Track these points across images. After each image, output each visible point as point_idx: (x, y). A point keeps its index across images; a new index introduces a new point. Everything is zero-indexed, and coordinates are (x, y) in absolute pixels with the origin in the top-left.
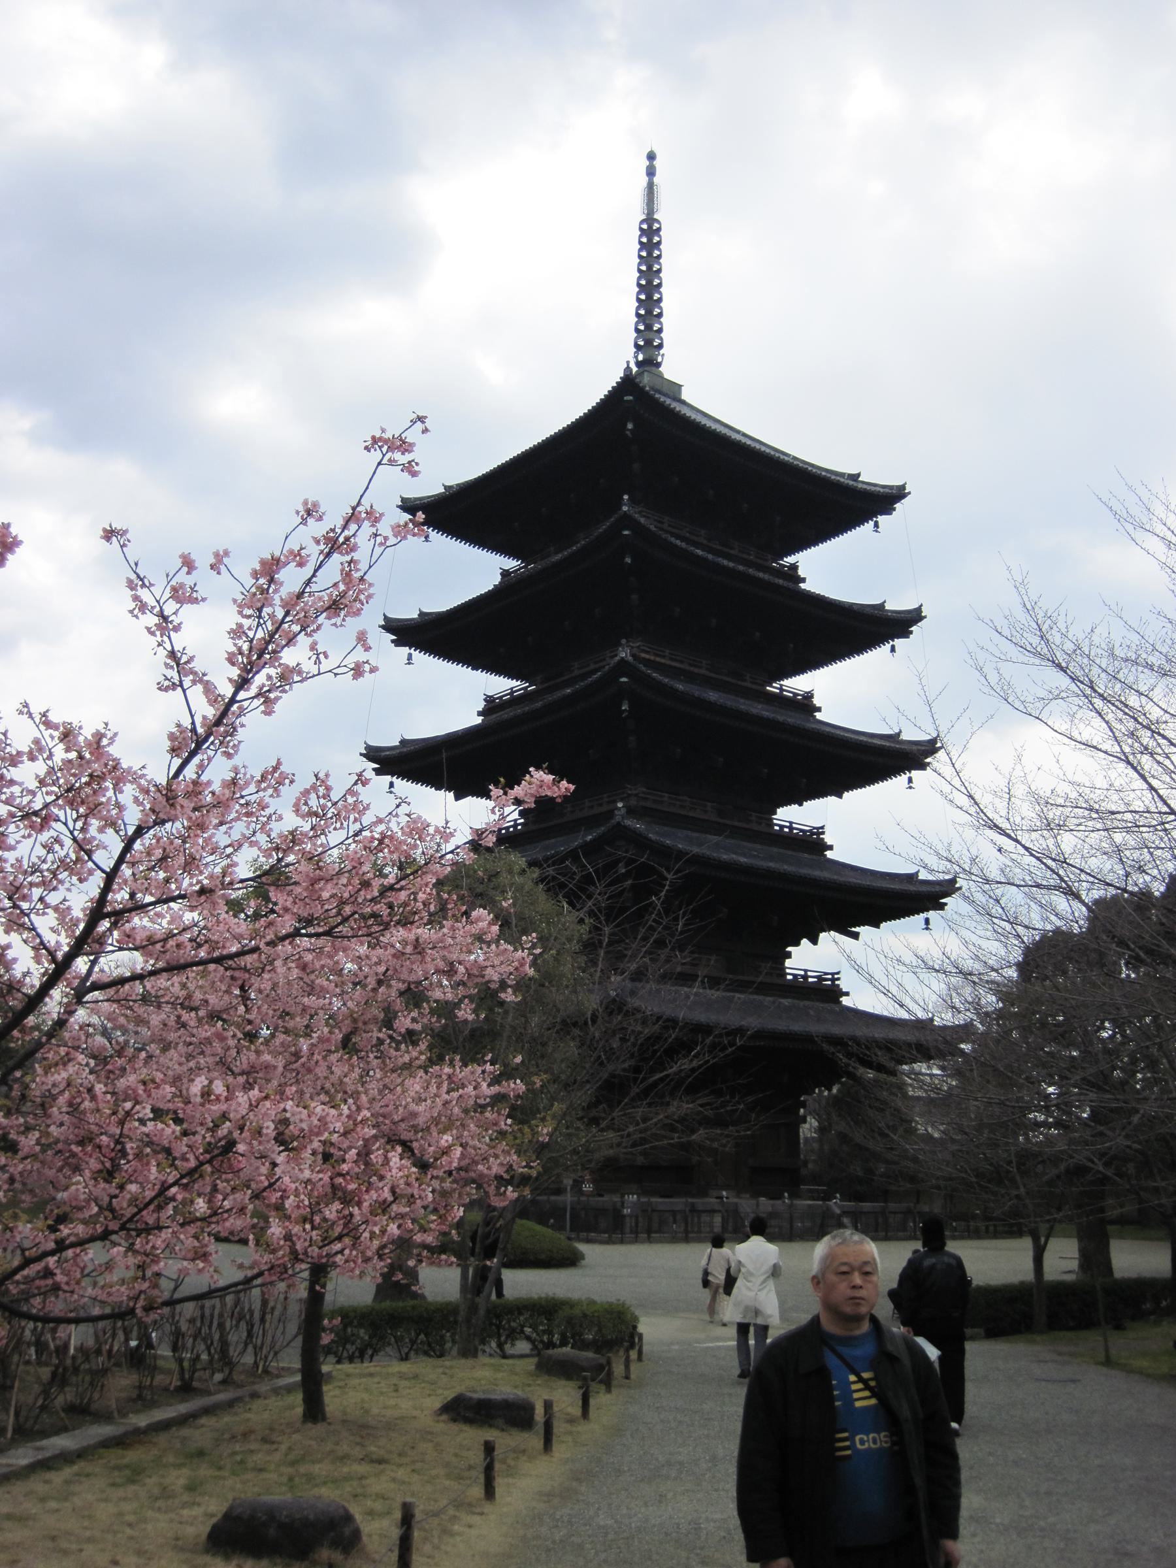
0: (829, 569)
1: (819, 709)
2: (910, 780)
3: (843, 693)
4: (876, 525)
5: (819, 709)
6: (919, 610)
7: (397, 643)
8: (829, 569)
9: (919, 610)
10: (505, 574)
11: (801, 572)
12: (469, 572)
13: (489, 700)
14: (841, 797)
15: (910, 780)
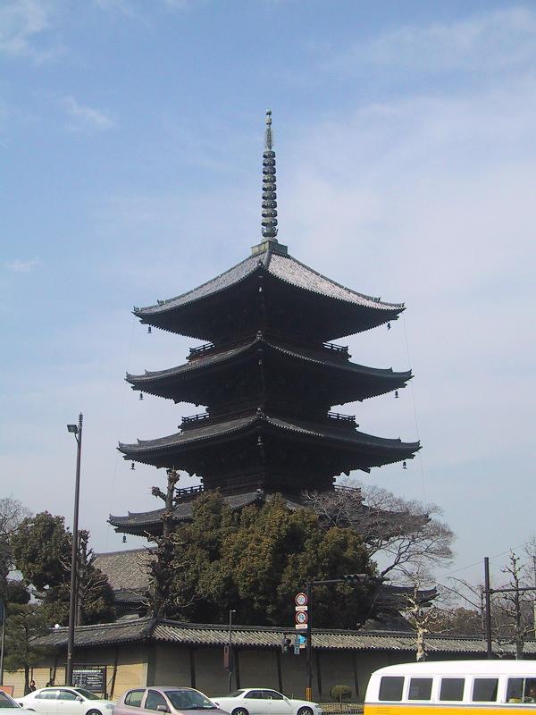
0: (364, 349)
1: (358, 426)
2: (405, 464)
3: (371, 416)
4: (389, 326)
5: (358, 426)
6: (410, 372)
7: (134, 388)
8: (364, 349)
9: (410, 372)
10: (192, 351)
11: (349, 352)
12: (174, 351)
13: (185, 419)
14: (369, 471)
15: (405, 464)
